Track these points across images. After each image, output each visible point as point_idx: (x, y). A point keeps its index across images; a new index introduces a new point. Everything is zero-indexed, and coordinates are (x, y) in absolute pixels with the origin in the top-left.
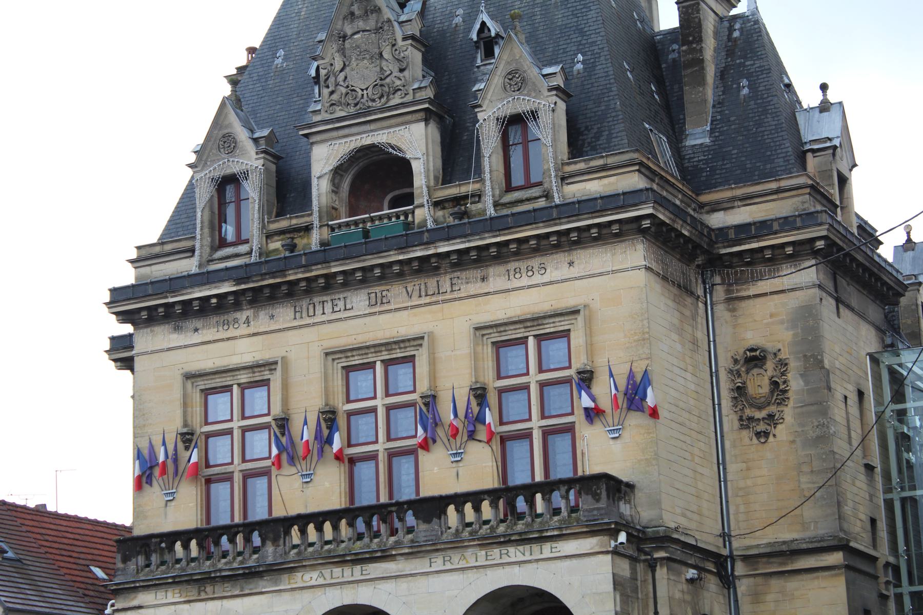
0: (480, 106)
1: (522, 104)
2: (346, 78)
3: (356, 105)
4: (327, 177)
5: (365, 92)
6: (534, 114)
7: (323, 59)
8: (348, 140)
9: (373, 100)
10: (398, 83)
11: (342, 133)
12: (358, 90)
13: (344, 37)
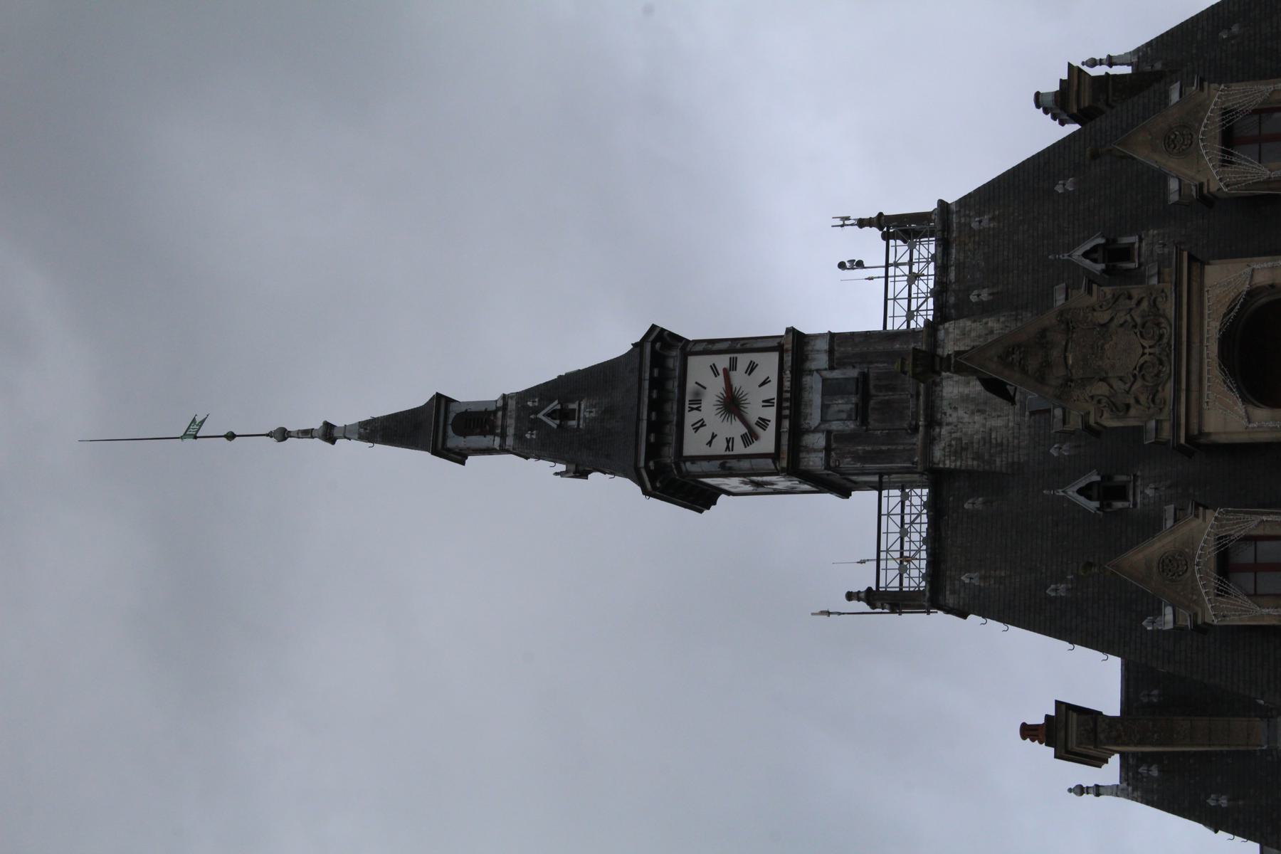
0: (1201, 185)
1: (1210, 125)
2: (1121, 379)
3: (1161, 363)
4: (1251, 409)
5: (1147, 351)
6: (1226, 112)
7: (1088, 413)
8: (1206, 375)
9: (1161, 336)
10: (1145, 304)
11: (1194, 386)
12: (1142, 361)
13: (1068, 381)
